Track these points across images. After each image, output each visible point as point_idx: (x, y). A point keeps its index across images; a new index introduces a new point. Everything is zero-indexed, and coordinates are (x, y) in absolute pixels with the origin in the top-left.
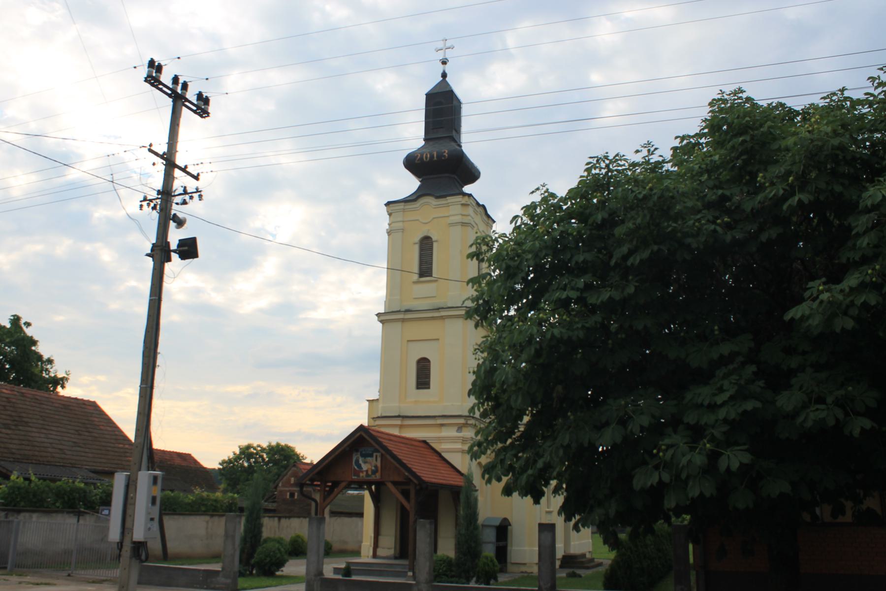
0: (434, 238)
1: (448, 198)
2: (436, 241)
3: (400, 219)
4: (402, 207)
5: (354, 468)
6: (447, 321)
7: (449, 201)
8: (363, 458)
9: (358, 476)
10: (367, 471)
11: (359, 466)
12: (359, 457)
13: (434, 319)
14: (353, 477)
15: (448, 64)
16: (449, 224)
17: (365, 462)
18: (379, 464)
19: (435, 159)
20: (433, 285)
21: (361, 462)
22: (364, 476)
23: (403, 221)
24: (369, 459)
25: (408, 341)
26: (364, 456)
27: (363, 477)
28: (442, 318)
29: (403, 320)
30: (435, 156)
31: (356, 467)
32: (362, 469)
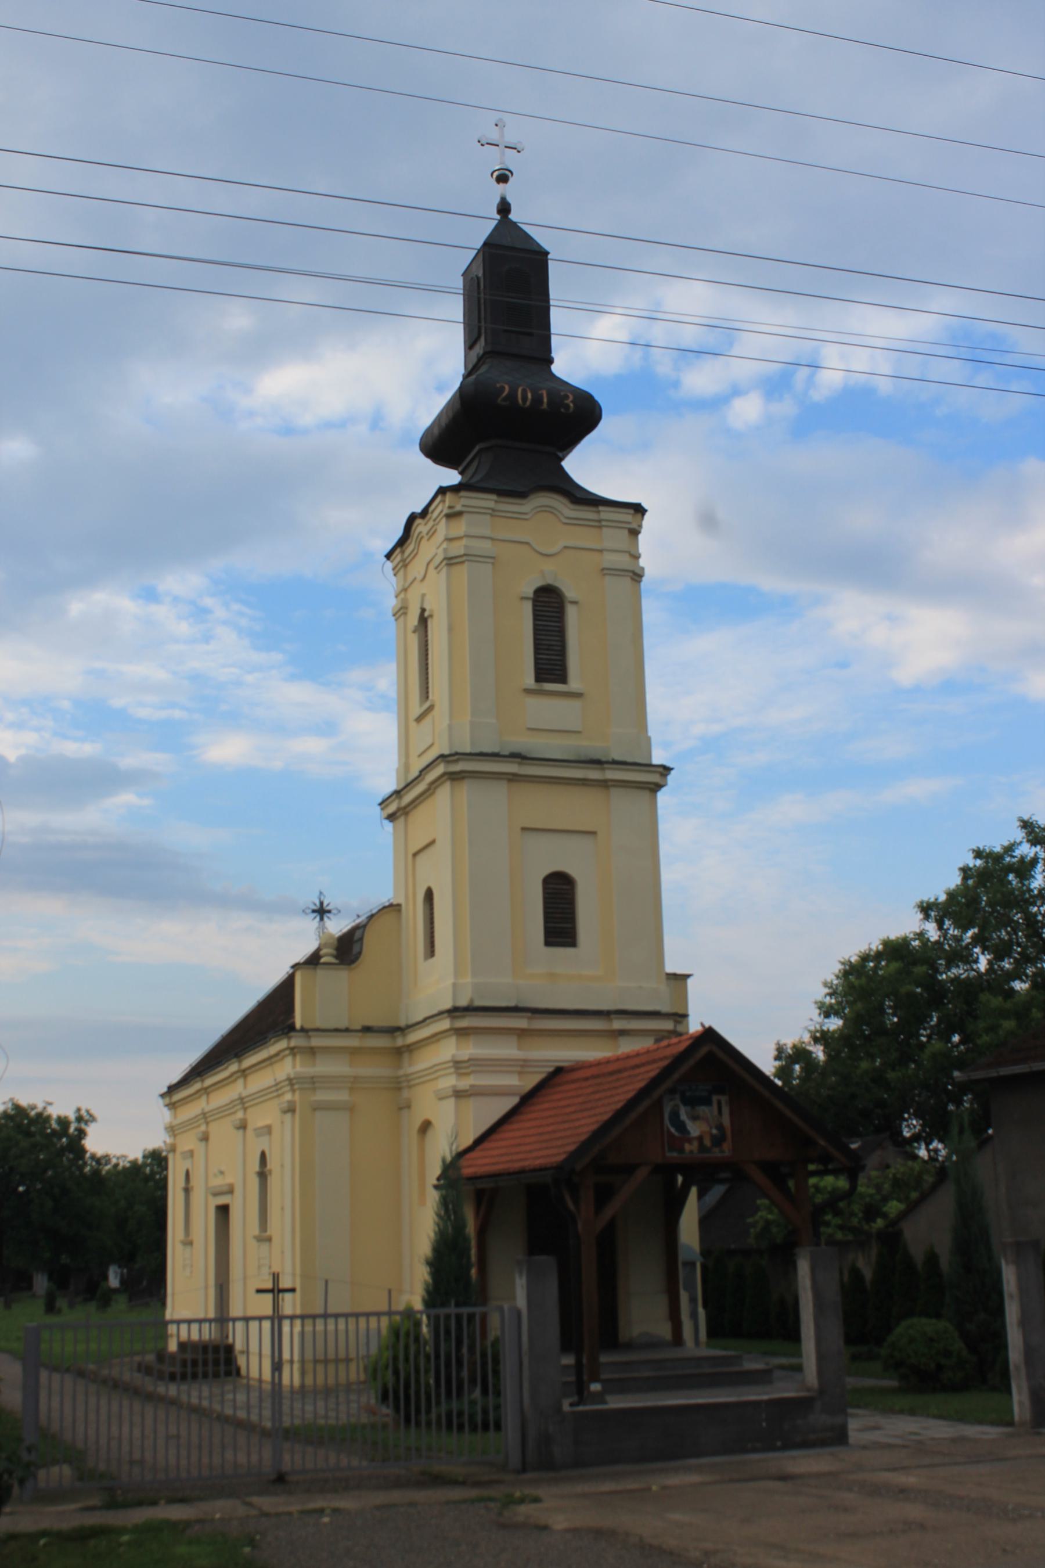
0: (569, 593)
1: (601, 508)
2: (575, 603)
3: (488, 533)
4: (491, 504)
5: (669, 1131)
6: (615, 793)
9: (681, 1150)
10: (700, 1139)
11: (681, 1127)
13: (584, 785)
14: (668, 1154)
16: (603, 569)
17: (695, 1118)
18: (726, 1120)
19: (545, 406)
20: (575, 704)
21: (683, 1116)
23: (492, 539)
24: (702, 1110)
25: (524, 829)
26: (691, 1102)
27: (691, 1152)
29: (513, 778)
30: (545, 400)
31: (673, 1130)
32: (689, 1133)
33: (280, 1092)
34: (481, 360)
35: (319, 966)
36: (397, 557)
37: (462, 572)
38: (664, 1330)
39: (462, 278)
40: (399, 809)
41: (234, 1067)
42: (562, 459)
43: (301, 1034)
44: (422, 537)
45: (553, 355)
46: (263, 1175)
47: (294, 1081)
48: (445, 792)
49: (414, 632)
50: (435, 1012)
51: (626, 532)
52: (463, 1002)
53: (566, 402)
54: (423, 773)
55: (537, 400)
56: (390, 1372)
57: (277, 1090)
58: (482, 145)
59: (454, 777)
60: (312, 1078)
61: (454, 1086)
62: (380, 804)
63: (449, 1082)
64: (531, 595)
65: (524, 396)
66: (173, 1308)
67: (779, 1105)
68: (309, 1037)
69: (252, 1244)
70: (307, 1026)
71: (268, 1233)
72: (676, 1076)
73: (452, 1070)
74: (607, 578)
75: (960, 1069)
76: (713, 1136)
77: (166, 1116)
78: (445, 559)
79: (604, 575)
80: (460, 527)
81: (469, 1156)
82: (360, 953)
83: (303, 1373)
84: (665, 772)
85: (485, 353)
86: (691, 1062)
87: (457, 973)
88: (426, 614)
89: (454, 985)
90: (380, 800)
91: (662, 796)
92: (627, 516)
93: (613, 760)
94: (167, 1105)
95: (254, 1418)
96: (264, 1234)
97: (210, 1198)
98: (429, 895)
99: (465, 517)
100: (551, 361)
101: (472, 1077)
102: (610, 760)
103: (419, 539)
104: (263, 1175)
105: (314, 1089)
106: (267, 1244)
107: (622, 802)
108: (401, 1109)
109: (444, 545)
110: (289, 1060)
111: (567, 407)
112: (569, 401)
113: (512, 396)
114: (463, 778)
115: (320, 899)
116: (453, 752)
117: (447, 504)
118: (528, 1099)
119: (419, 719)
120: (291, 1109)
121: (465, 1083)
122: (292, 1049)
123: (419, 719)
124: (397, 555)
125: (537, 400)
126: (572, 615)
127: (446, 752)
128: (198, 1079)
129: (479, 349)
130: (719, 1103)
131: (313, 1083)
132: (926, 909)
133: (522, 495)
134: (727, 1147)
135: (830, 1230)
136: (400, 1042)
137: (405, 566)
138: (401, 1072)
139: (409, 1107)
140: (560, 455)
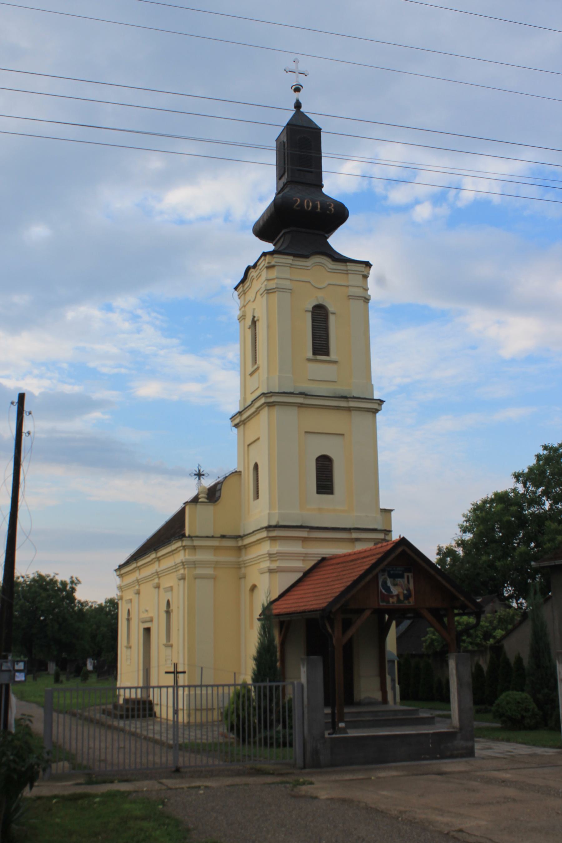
0: (331, 309)
1: (348, 264)
3: (288, 276)
5: (381, 591)
7: (349, 268)
8: (392, 580)
9: (388, 602)
10: (398, 596)
11: (388, 589)
12: (386, 578)
13: (338, 409)
14: (381, 604)
15: (302, 90)
16: (349, 296)
17: (395, 585)
18: (412, 586)
19: (319, 210)
21: (389, 584)
22: (395, 602)
23: (291, 280)
24: (399, 581)
25: (306, 432)
27: (393, 603)
28: (349, 409)
29: (300, 406)
30: (319, 207)
31: (383, 591)
32: (392, 592)
33: (177, 569)
34: (285, 185)
35: (199, 503)
36: (241, 289)
37: (275, 297)
38: (378, 696)
39: (275, 142)
40: (240, 421)
41: (153, 556)
42: (327, 238)
43: (189, 539)
44: (254, 279)
45: (323, 183)
46: (168, 612)
47: (185, 563)
48: (265, 412)
49: (249, 328)
50: (259, 528)
51: (361, 276)
52: (274, 523)
53: (330, 208)
54: (254, 402)
55: (315, 207)
56: (235, 715)
57: (176, 568)
58: (287, 72)
59: (270, 405)
60: (194, 562)
61: (268, 567)
62: (231, 419)
63: (266, 565)
64: (311, 309)
65: (308, 204)
66: (121, 681)
67: (440, 578)
68: (193, 540)
69: (163, 648)
70: (192, 535)
71: (171, 642)
72: (385, 563)
73: (268, 558)
74: (351, 300)
75: (534, 561)
76: (404, 595)
77: (118, 581)
78: (265, 290)
79: (349, 299)
80: (274, 273)
81: (276, 603)
82: (220, 497)
83: (189, 716)
84: (380, 403)
85: (287, 182)
86: (393, 555)
87: (271, 507)
88: (256, 319)
89: (269, 514)
90: (231, 417)
91: (379, 416)
92: (361, 268)
93: (353, 396)
94: (118, 576)
95: (164, 739)
96: (169, 643)
97: (141, 624)
98: (256, 467)
99: (276, 268)
100: (322, 186)
101: (278, 562)
102: (352, 396)
103: (252, 279)
104: (168, 612)
105: (195, 568)
106: (170, 648)
107: (358, 419)
108: (240, 578)
109: (265, 283)
110: (182, 552)
111: (330, 210)
112: (332, 207)
113: (302, 204)
114: (274, 405)
115: (199, 468)
116: (269, 391)
117: (267, 261)
118: (307, 574)
119: (251, 374)
120: (183, 578)
121: (274, 565)
122: (184, 547)
123: (251, 374)
124: (241, 288)
125: (315, 207)
126: (332, 319)
127: (266, 392)
128: (134, 562)
129: (284, 180)
130: (408, 577)
131: (194, 564)
132: (517, 476)
133: (306, 257)
134: (412, 600)
135: (465, 645)
136: (240, 543)
137: (245, 294)
138: (241, 559)
139: (245, 577)
140: (327, 235)
